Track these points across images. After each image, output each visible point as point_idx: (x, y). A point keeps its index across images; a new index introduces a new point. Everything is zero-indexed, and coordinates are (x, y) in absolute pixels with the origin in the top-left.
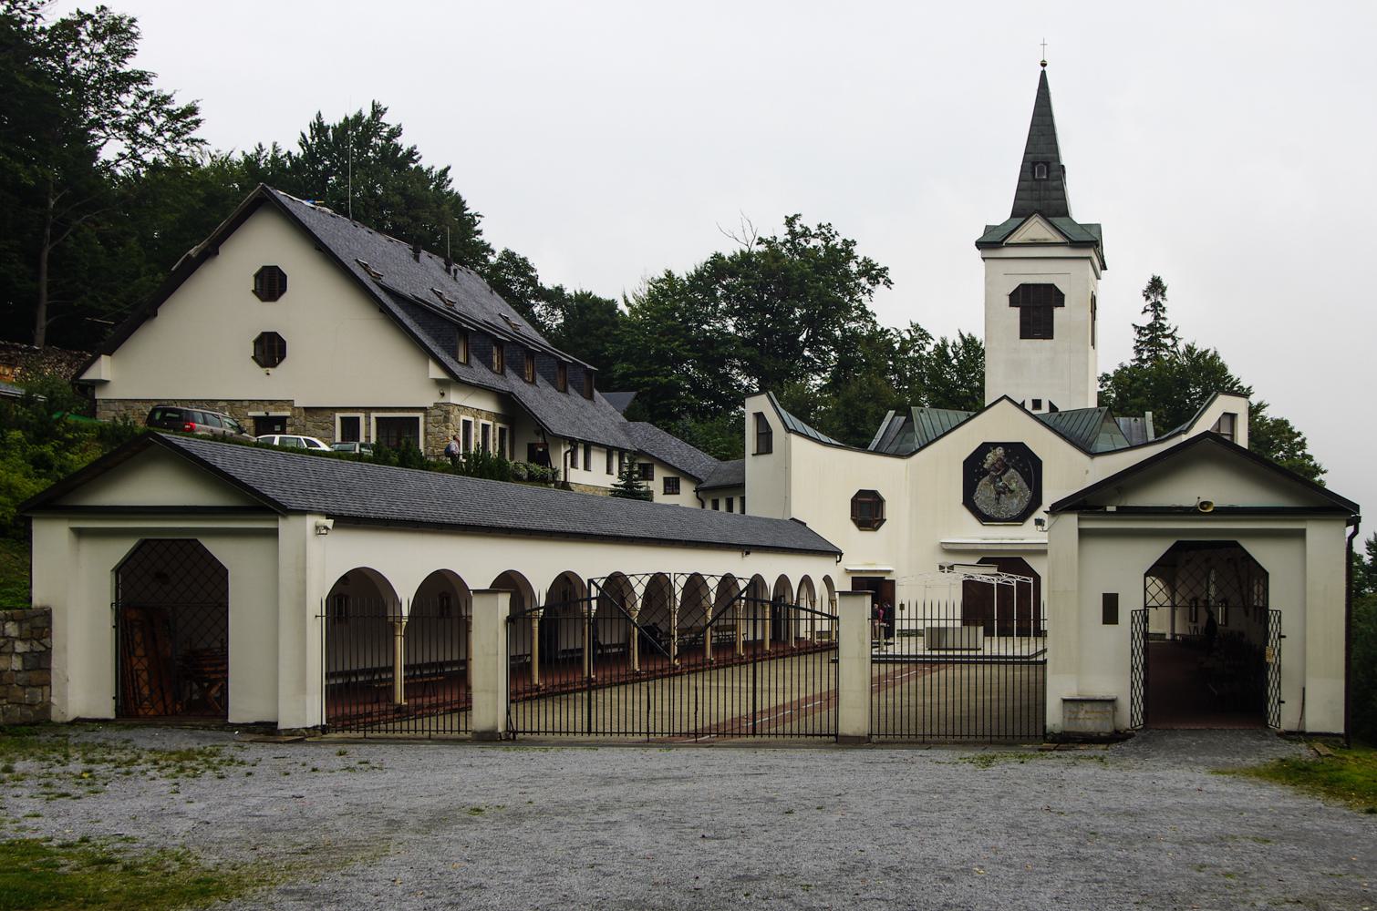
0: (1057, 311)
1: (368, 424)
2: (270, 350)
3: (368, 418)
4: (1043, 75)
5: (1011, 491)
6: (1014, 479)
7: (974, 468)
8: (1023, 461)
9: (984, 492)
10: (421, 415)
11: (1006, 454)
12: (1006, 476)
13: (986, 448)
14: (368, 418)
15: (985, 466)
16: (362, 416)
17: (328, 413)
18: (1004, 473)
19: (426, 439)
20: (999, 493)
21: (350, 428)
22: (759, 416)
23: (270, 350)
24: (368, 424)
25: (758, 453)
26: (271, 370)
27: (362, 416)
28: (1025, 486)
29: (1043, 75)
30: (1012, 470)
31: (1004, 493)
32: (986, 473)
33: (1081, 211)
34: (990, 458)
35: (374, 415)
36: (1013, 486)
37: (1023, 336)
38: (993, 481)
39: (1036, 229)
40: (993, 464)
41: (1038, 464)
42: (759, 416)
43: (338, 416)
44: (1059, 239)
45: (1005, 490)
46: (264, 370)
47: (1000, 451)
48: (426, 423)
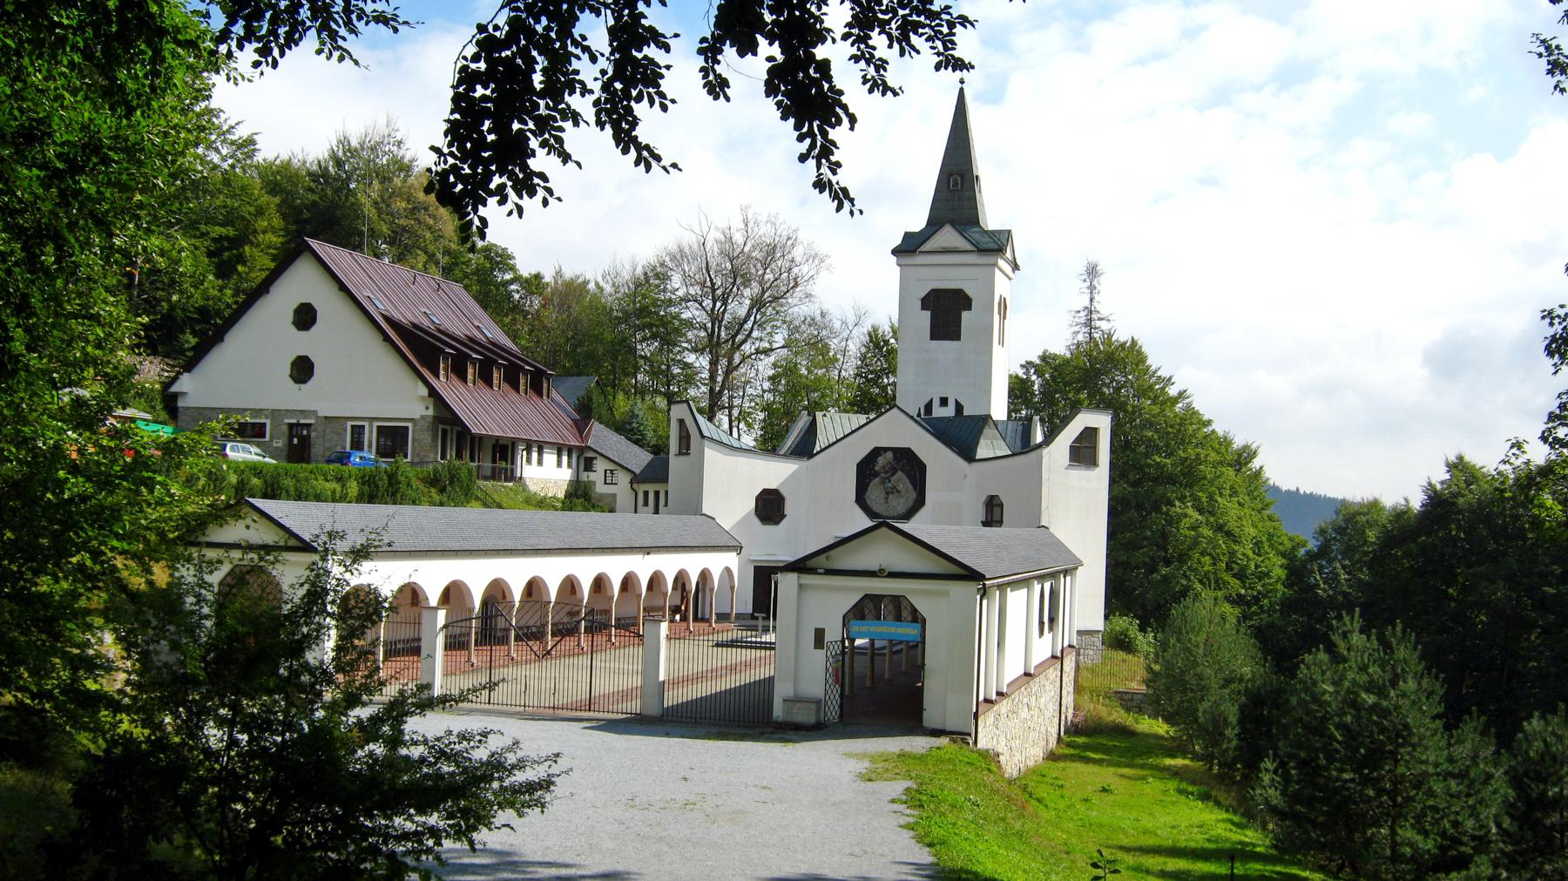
0: (965, 315)
1: (371, 432)
2: (302, 370)
3: (371, 426)
4: (961, 92)
5: (899, 492)
6: (901, 481)
7: (866, 470)
8: (909, 465)
9: (875, 494)
10: (410, 425)
11: (895, 458)
12: (895, 477)
13: (877, 452)
14: (371, 426)
15: (876, 468)
16: (366, 424)
17: (342, 421)
18: (893, 475)
19: (413, 445)
20: (887, 493)
21: (358, 431)
22: (681, 422)
23: (302, 370)
24: (371, 432)
25: (680, 454)
26: (302, 386)
27: (366, 424)
28: (910, 487)
29: (961, 92)
30: (900, 473)
31: (892, 493)
32: (876, 474)
33: (993, 216)
34: (881, 461)
35: (376, 424)
36: (900, 487)
37: (931, 339)
38: (883, 482)
39: (948, 236)
40: (883, 467)
41: (922, 468)
42: (681, 422)
43: (350, 423)
44: (969, 247)
45: (894, 491)
46: (297, 386)
47: (889, 455)
48: (413, 431)
